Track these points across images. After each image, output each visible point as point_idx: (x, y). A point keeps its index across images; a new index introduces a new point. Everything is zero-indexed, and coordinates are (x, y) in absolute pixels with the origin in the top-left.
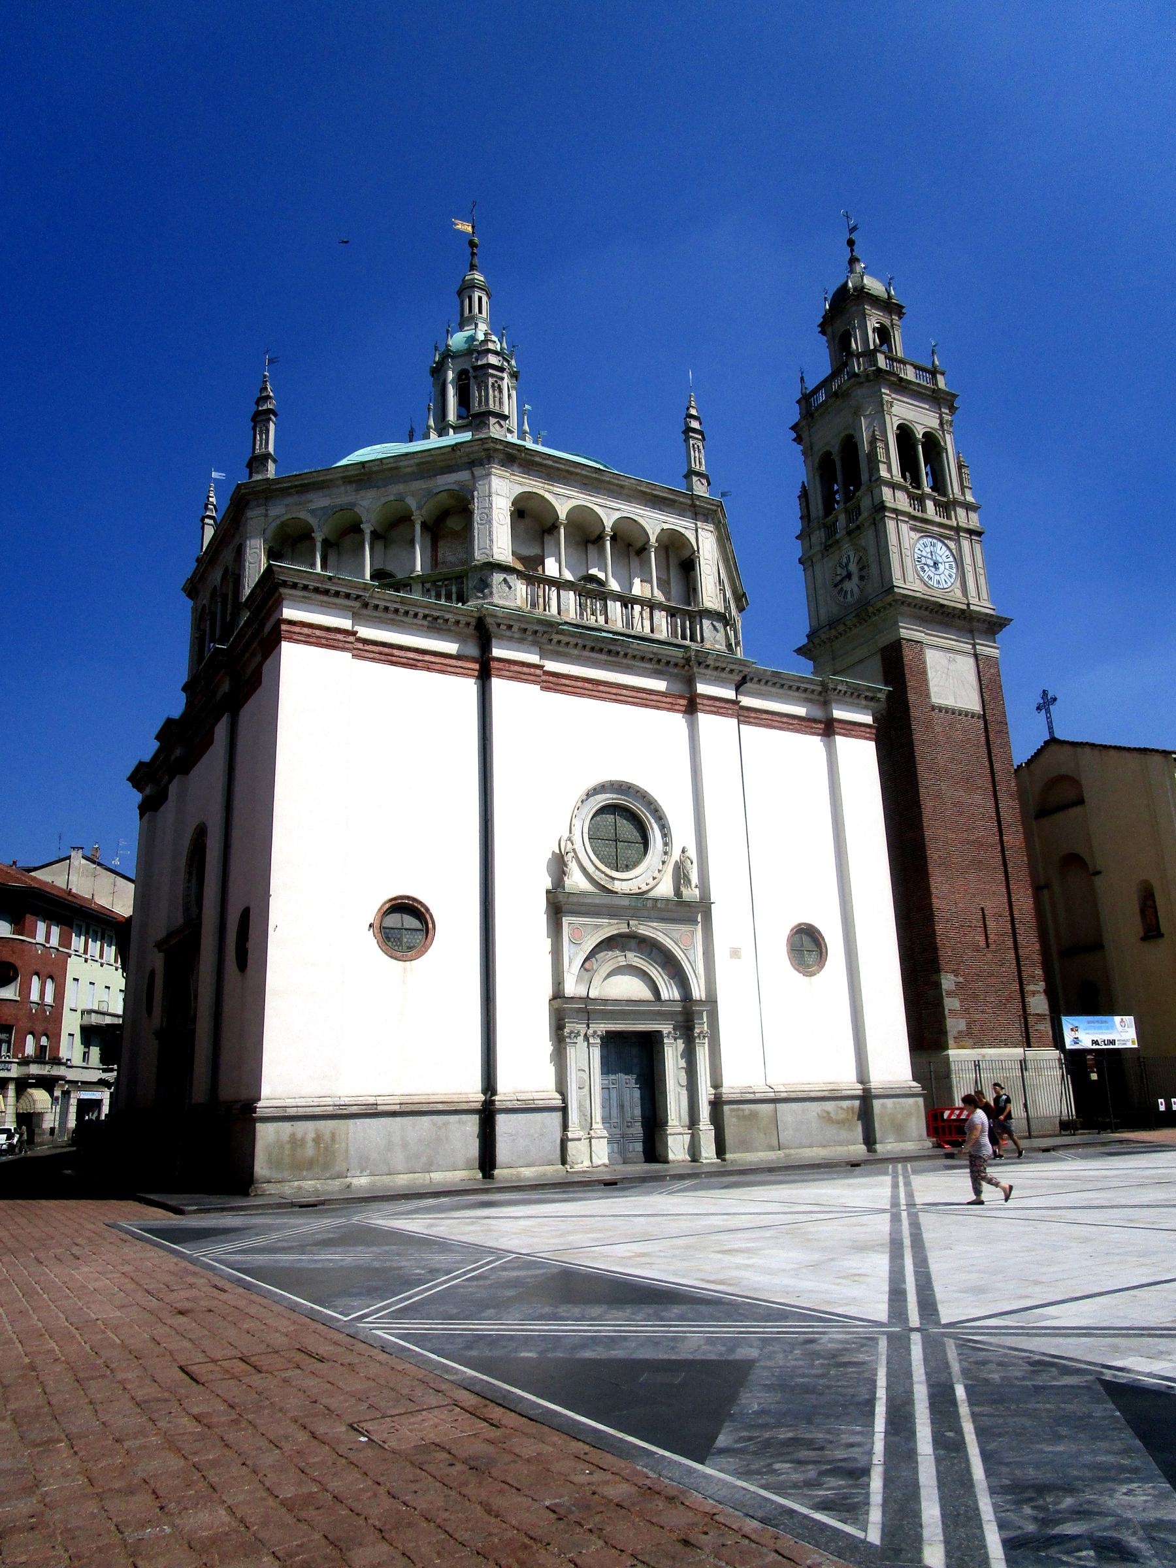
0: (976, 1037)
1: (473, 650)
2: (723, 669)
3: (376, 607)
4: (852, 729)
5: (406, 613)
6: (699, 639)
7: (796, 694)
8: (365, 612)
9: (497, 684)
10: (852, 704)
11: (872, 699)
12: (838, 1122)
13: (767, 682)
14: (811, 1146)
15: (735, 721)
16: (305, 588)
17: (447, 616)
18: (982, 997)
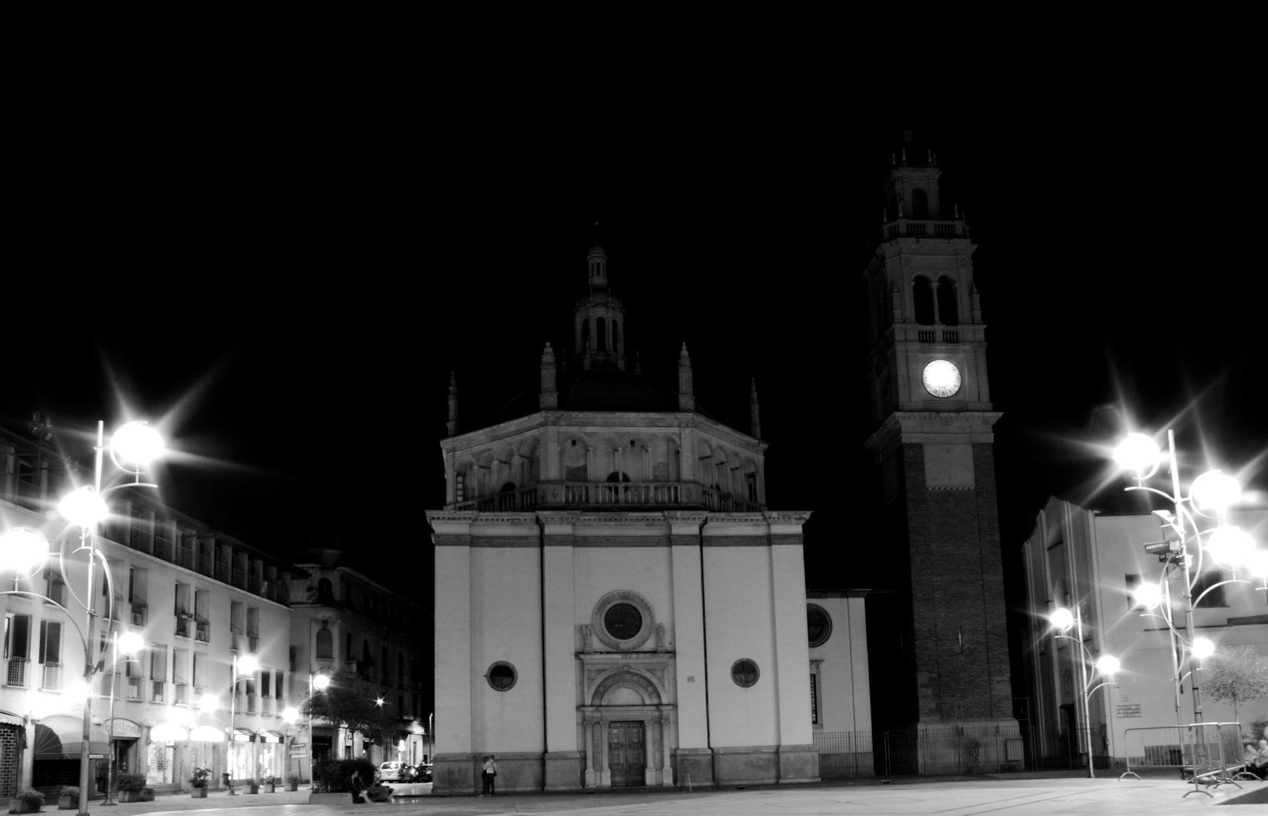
0: (944, 713)
1: (535, 531)
2: (689, 518)
3: (482, 520)
4: (785, 539)
5: (498, 520)
6: (679, 500)
7: (745, 523)
8: (477, 523)
9: (547, 549)
10: (786, 524)
11: (800, 519)
12: (759, 767)
13: (723, 520)
14: (738, 780)
15: (698, 547)
16: (444, 518)
17: (520, 518)
18: (953, 686)
